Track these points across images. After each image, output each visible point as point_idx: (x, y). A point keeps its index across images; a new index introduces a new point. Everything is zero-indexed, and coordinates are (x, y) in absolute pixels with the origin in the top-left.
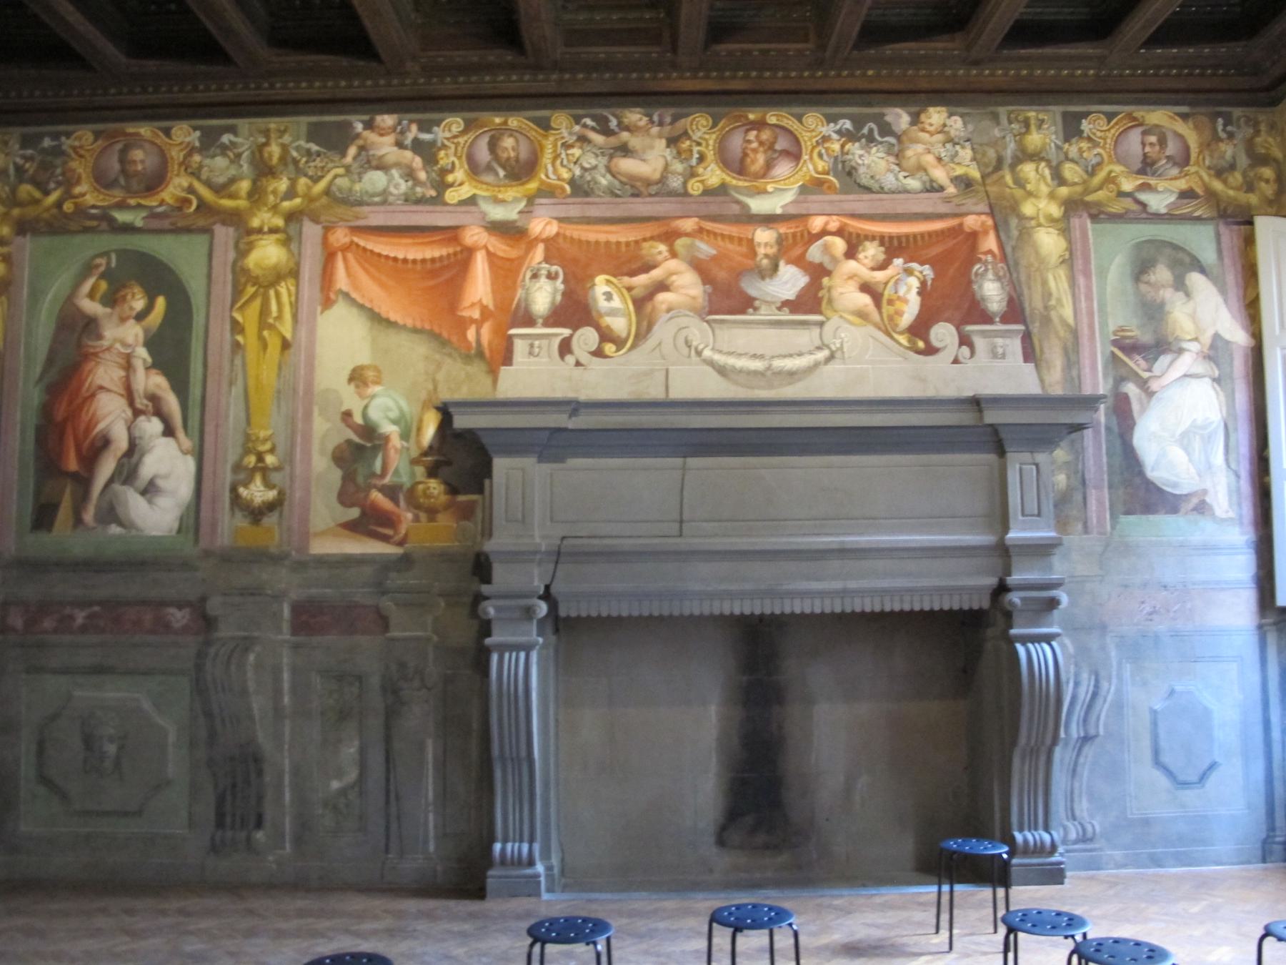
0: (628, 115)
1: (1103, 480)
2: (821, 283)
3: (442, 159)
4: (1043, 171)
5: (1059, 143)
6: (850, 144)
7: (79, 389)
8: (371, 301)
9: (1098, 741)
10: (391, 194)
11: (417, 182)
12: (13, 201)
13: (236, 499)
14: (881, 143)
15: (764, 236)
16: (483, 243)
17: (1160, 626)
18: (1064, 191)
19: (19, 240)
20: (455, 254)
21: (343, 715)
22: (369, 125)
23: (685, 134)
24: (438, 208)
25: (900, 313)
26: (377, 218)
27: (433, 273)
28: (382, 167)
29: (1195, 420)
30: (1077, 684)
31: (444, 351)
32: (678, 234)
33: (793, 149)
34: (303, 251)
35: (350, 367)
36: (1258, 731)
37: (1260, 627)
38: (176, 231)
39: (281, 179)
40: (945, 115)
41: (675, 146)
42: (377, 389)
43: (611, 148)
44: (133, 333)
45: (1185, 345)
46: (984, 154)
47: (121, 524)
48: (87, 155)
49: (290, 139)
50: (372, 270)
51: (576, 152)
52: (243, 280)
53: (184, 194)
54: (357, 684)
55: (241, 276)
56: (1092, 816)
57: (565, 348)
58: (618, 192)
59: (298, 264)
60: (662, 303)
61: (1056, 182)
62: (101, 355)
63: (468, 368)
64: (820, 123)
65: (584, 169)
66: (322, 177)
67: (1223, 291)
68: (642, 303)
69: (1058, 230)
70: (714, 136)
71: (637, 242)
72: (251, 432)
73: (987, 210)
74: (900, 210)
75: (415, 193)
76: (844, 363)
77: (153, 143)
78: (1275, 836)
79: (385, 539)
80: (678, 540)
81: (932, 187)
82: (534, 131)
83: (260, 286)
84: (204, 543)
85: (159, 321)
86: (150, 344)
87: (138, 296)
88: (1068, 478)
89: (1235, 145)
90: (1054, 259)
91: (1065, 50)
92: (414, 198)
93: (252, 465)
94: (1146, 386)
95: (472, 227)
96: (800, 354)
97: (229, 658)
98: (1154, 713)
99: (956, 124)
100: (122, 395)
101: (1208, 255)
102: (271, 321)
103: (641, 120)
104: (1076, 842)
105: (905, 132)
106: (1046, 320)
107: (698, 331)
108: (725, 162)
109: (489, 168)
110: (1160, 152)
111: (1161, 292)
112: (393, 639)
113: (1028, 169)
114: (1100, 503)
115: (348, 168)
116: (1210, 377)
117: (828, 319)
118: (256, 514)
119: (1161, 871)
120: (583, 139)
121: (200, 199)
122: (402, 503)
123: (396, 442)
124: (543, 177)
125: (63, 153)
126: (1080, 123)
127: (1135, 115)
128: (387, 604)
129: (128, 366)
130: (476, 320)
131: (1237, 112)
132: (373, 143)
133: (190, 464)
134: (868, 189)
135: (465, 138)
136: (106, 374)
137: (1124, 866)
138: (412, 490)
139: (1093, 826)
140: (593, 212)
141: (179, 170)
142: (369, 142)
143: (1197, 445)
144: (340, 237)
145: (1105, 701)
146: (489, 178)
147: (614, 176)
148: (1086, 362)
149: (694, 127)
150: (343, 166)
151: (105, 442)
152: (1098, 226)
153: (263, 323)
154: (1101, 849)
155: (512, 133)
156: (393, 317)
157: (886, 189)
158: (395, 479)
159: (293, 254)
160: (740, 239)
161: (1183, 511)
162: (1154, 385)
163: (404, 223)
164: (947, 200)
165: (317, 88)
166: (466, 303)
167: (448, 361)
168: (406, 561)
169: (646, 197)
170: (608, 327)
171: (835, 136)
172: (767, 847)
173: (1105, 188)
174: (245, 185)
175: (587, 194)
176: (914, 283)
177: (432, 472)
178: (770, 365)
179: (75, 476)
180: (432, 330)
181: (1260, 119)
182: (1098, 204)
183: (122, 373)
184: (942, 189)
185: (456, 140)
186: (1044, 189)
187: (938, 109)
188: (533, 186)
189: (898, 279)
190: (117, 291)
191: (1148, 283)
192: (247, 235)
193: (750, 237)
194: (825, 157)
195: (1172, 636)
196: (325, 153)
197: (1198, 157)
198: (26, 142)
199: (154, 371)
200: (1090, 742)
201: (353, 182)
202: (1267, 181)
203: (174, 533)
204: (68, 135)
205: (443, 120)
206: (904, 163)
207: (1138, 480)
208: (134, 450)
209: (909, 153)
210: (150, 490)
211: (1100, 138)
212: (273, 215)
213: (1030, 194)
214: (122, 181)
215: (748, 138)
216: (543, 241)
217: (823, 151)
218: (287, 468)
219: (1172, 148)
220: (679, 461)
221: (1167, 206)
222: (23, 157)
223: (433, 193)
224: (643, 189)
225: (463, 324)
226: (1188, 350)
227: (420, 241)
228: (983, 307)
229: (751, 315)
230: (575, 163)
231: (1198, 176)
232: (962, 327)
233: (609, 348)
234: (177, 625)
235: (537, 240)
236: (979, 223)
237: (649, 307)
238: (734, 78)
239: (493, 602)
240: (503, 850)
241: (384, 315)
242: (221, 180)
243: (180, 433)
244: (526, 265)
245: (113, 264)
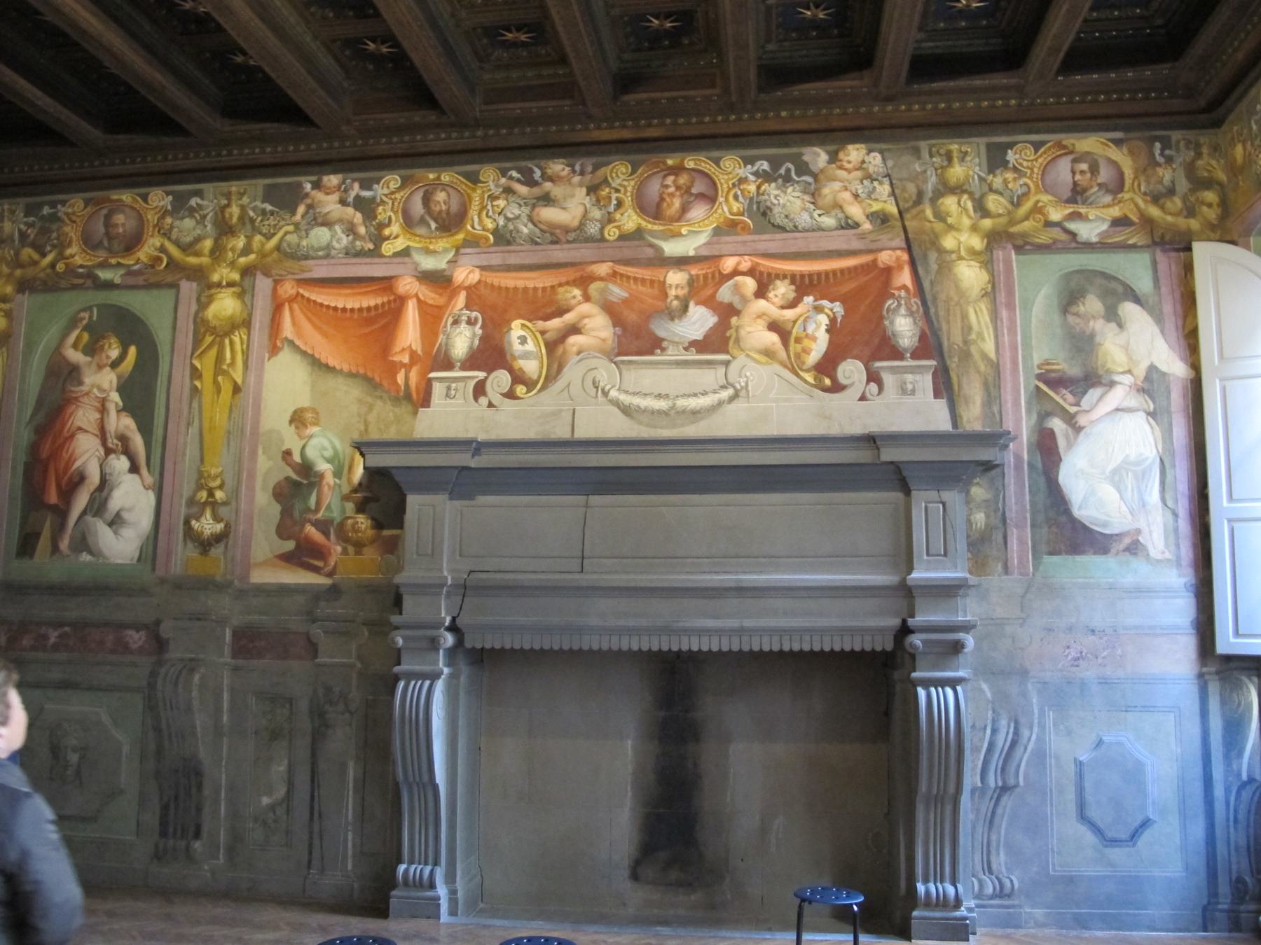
0: (551, 164)
1: (1026, 518)
2: (730, 322)
3: (380, 214)
4: (965, 202)
5: (983, 175)
6: (766, 185)
7: (61, 431)
8: (313, 348)
9: (1018, 790)
10: (334, 249)
11: (357, 236)
12: (17, 263)
13: (189, 532)
14: (798, 182)
15: (676, 278)
16: (415, 292)
17: (1089, 672)
18: (987, 223)
19: (20, 296)
20: (389, 302)
21: (275, 735)
22: (317, 185)
23: (605, 182)
24: (376, 260)
25: (807, 351)
26: (320, 271)
27: (369, 321)
28: (327, 224)
29: (1127, 456)
30: (994, 731)
31: (376, 393)
32: (593, 278)
33: (710, 193)
34: (255, 302)
35: (293, 409)
36: (1197, 788)
37: (1201, 676)
38: (149, 286)
39: (239, 237)
40: (864, 151)
41: (595, 193)
42: (314, 430)
43: (535, 198)
44: (108, 379)
45: (1117, 378)
46: (904, 190)
47: (90, 552)
48: (78, 220)
49: (248, 200)
50: (314, 319)
51: (501, 203)
52: (202, 330)
53: (156, 253)
54: (288, 706)
55: (202, 327)
56: (1009, 870)
57: (480, 390)
58: (538, 240)
59: (250, 315)
60: (573, 345)
61: (979, 214)
62: (81, 399)
63: (397, 410)
64: (737, 166)
65: (508, 219)
66: (274, 234)
67: (1159, 319)
68: (554, 345)
69: (980, 263)
70: (632, 183)
71: (552, 287)
72: (203, 469)
73: (903, 245)
74: (813, 248)
75: (354, 247)
76: (748, 402)
77: (132, 208)
78: (1218, 903)
79: (316, 570)
80: (577, 576)
81: (847, 224)
82: (463, 184)
83: (217, 336)
84: (160, 572)
85: (130, 368)
86: (121, 389)
87: (114, 346)
88: (988, 517)
89: (1174, 170)
90: (975, 292)
91: (978, 82)
92: (353, 251)
93: (203, 500)
94: (1074, 421)
95: (406, 277)
96: (704, 394)
97: (178, 677)
98: (1079, 765)
99: (875, 160)
100: (97, 436)
101: (1143, 283)
102: (225, 367)
103: (564, 169)
104: (992, 897)
105: (822, 171)
106: (966, 355)
107: (605, 372)
108: (642, 207)
109: (422, 221)
110: (1091, 179)
111: (1091, 323)
112: (319, 665)
113: (950, 203)
114: (1022, 542)
115: (297, 225)
116: (1146, 412)
117: (734, 358)
118: (205, 545)
119: (1087, 934)
120: (508, 191)
121: (169, 257)
122: (332, 537)
123: (329, 479)
124: (469, 227)
125: (59, 219)
126: (1006, 153)
127: (1064, 143)
128: (317, 631)
129: (103, 410)
131: (1176, 135)
132: (320, 201)
133: (151, 497)
134: (782, 229)
135: (402, 194)
136: (84, 416)
137: (1044, 925)
138: (341, 525)
139: (1012, 881)
140: (513, 260)
141: (153, 231)
142: (316, 201)
143: (1130, 482)
144: (288, 289)
145: (1026, 749)
146: (421, 231)
147: (535, 225)
148: (1008, 397)
149: (614, 175)
150: (292, 224)
151: (81, 478)
152: (1021, 257)
153: (218, 370)
154: (1020, 906)
155: (444, 187)
156: (331, 363)
157: (800, 228)
158: (327, 514)
159: (246, 306)
160: (652, 282)
161: (1113, 551)
162: (1082, 420)
164: (862, 237)
165: (267, 154)
166: (397, 349)
167: (379, 403)
168: (334, 591)
169: (565, 243)
170: (521, 369)
171: (752, 178)
172: (680, 884)
173: (1031, 219)
174: (208, 244)
175: (509, 243)
176: (823, 320)
177: (360, 509)
178: (674, 405)
179: (54, 509)
180: (365, 374)
181: (1202, 140)
182: (1023, 235)
183: (98, 416)
184: (857, 225)
185: (393, 197)
186: (966, 222)
187: (857, 146)
188: (460, 236)
189: (808, 317)
190: (97, 341)
191: (1077, 314)
192: (208, 289)
193: (662, 279)
194: (741, 199)
195: (1101, 683)
196: (278, 212)
197: (1133, 184)
198: (30, 210)
199: (124, 414)
200: (1009, 792)
201: (301, 238)
202: (1210, 205)
203: (135, 561)
204: (64, 203)
205: (383, 178)
206: (820, 202)
207: (1063, 519)
208: (105, 484)
209: (826, 191)
210: (116, 522)
211: (1028, 167)
212: (230, 272)
213: (951, 227)
214: (106, 243)
215: (665, 183)
217: (739, 193)
218: (234, 504)
219: (1105, 175)
220: (581, 499)
221: (1099, 234)
222: (26, 224)
223: (371, 246)
224: (561, 237)
225: (393, 368)
226: (1120, 383)
228: (893, 343)
229: (659, 355)
230: (500, 214)
231: (1133, 202)
232: (870, 363)
233: (520, 390)
234: (134, 646)
235: (460, 287)
236: (894, 259)
237: (560, 350)
238: (649, 125)
239: (402, 632)
240: (406, 871)
241: (323, 361)
242: (188, 239)
243: (144, 471)
244: (448, 313)
245: (95, 318)
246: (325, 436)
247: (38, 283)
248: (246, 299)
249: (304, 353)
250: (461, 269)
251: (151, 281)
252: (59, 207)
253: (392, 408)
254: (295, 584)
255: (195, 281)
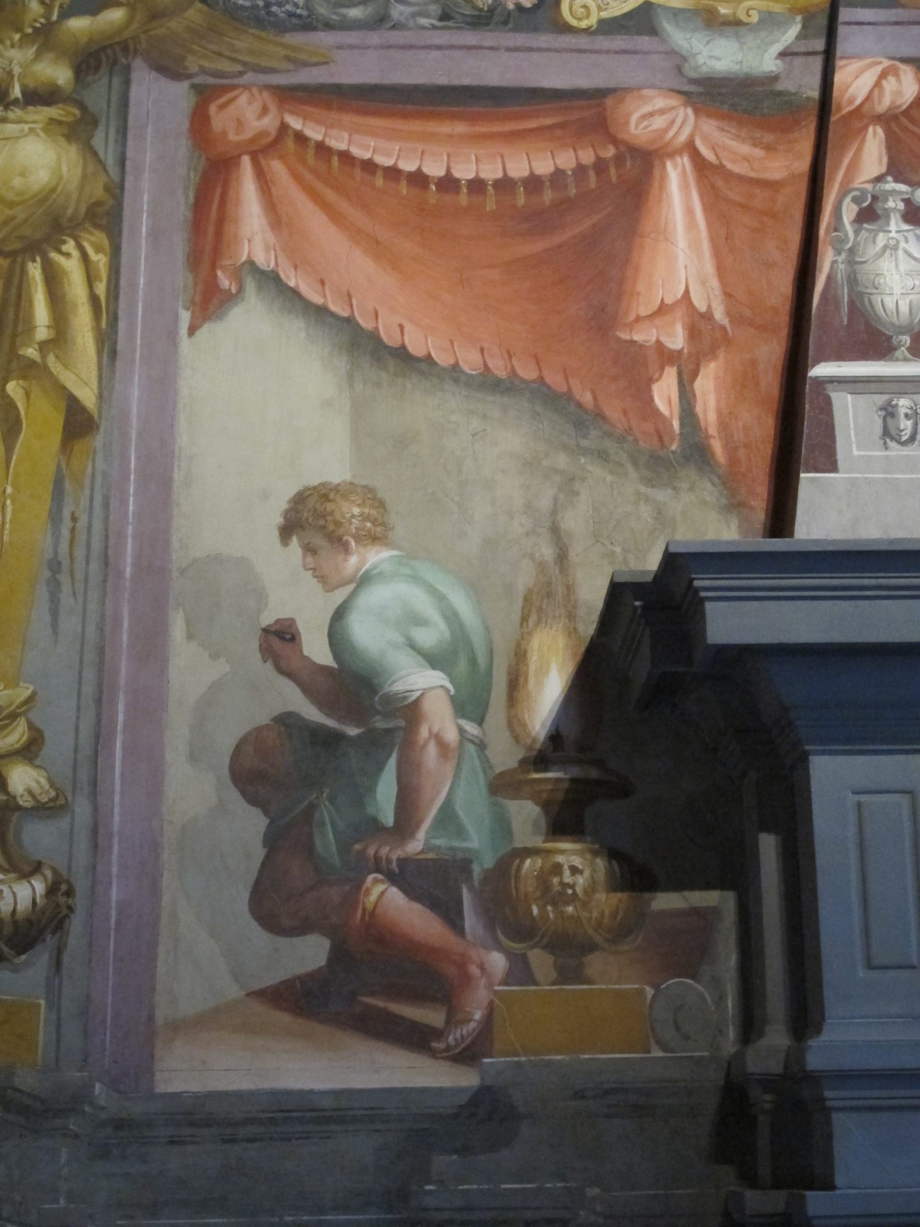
16: (683, 138)
20: (600, 166)
24: (544, 40)
31: (585, 443)
34: (130, 153)
35: (292, 492)
59: (116, 190)
63: (661, 495)
95: (647, 92)
102: (31, 352)
130: (680, 352)
156: (416, 345)
159: (101, 163)
163: (442, 80)
167: (596, 470)
212: (38, 55)
216: (878, 119)
218: (82, 809)
227: (497, 128)
241: (390, 338)
246: (415, 578)
248: (98, 141)
249: (321, 312)
250: (854, 66)
253: (643, 489)
254: (338, 1094)
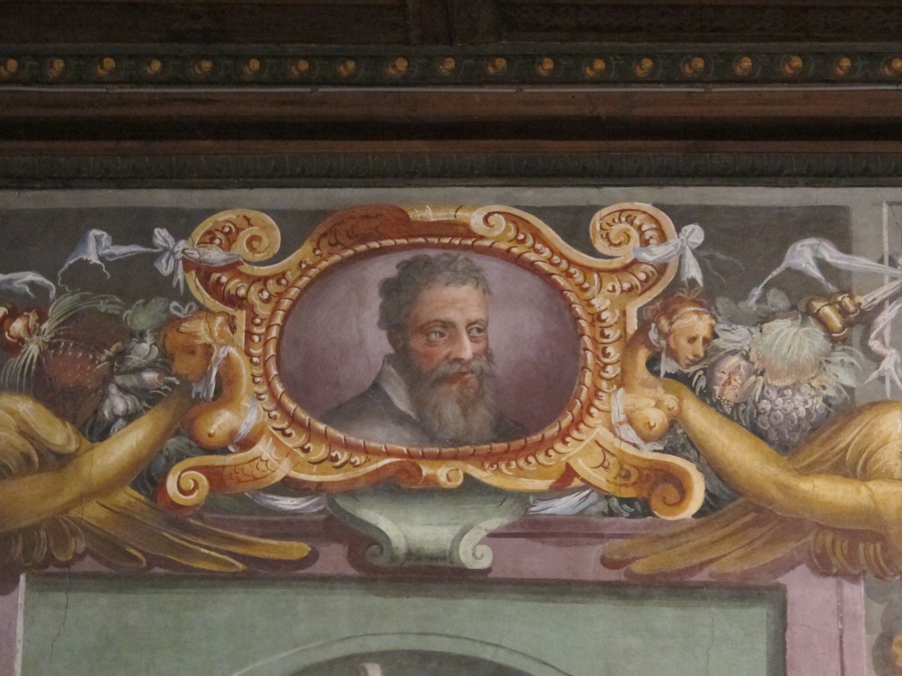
53: (648, 453)
77: (518, 261)
214: (401, 401)
247: (79, 544)
251: (638, 567)
252: (161, 235)
255: (854, 579)
